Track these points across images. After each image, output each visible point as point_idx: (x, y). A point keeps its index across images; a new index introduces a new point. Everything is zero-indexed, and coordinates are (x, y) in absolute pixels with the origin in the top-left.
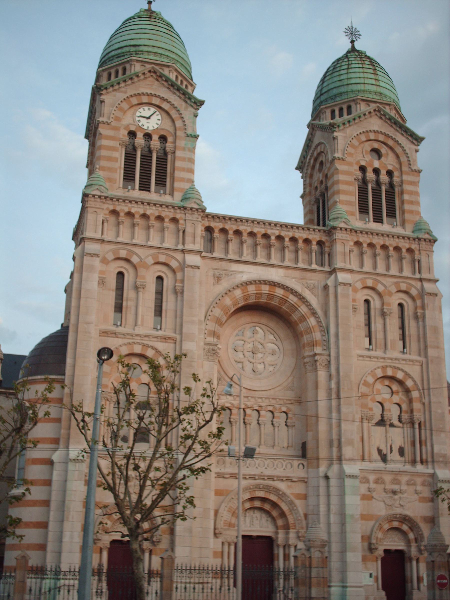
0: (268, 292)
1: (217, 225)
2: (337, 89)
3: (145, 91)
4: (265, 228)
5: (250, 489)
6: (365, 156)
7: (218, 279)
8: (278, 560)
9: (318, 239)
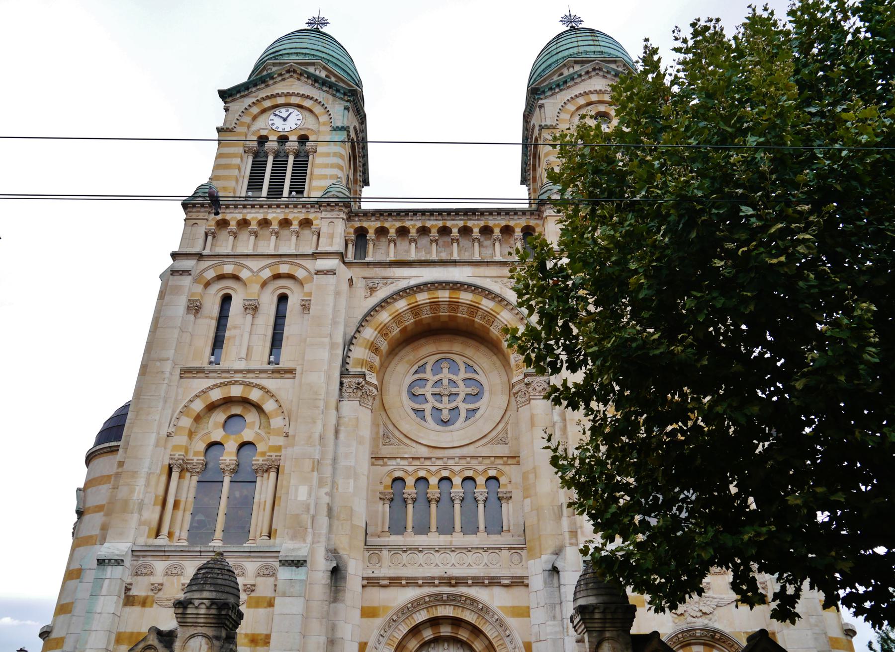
3: (280, 92)
5: (426, 602)
7: (372, 290)
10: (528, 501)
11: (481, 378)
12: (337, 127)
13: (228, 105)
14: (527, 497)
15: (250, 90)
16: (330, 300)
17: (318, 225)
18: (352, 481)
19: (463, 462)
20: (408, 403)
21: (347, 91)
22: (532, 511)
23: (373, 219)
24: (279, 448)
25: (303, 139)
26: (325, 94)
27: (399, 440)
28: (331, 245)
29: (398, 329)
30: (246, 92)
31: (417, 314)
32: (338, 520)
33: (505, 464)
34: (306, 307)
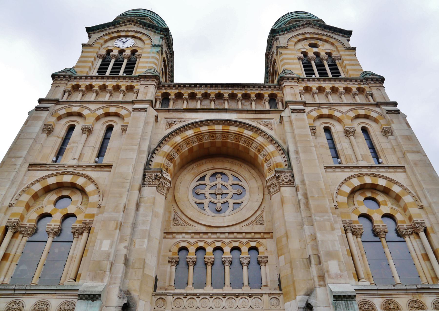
4: (218, 89)
7: (171, 125)
10: (282, 258)
11: (244, 184)
12: (155, 45)
14: (281, 255)
15: (105, 29)
16: (141, 125)
18: (146, 240)
19: (231, 236)
20: (192, 198)
21: (162, 29)
22: (285, 264)
23: (174, 88)
24: (93, 216)
26: (149, 32)
27: (185, 222)
29: (187, 148)
30: (103, 30)
31: (200, 139)
32: (133, 268)
33: (263, 238)
34: (124, 130)
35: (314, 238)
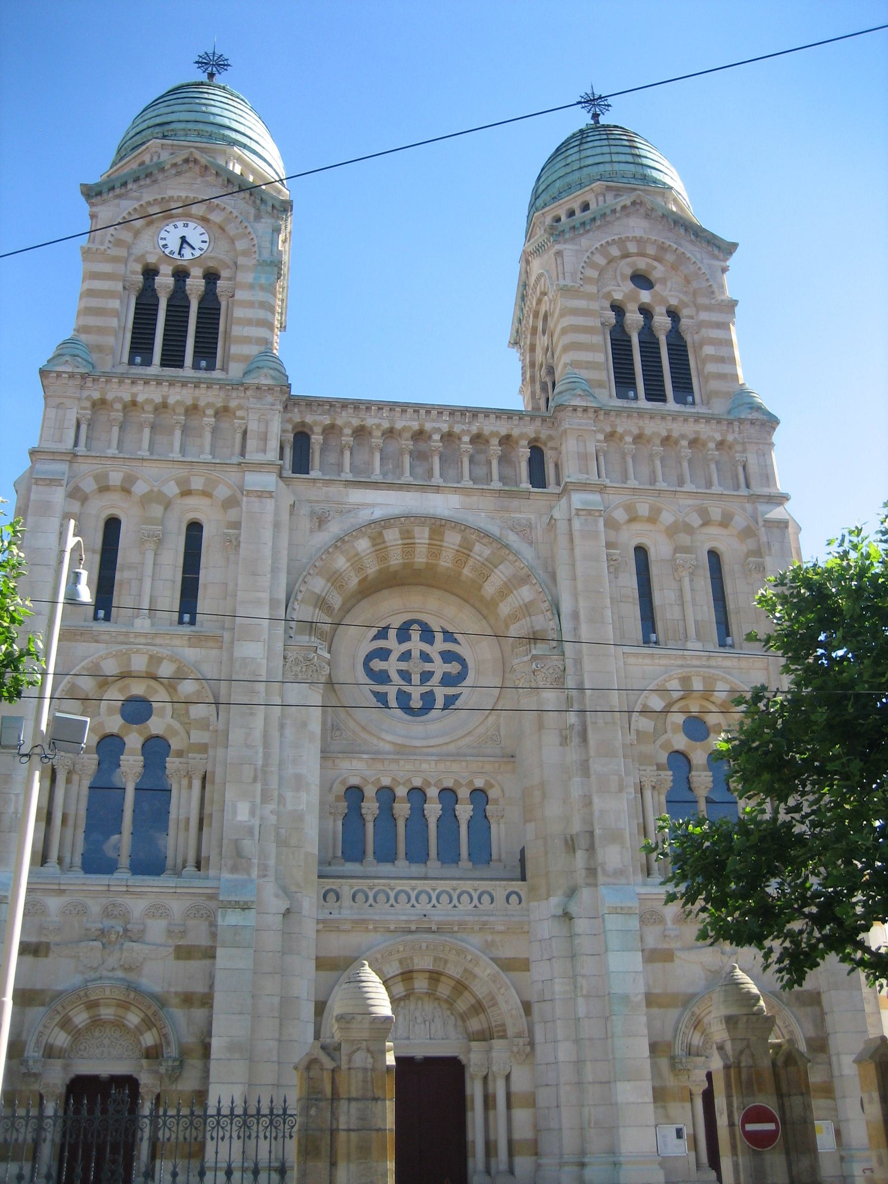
0: (427, 541)
1: (317, 420)
2: (561, 179)
6: (620, 283)
8: (473, 1109)
9: (533, 435)
10: (531, 826)
13: (95, 209)
14: (531, 821)
17: (242, 418)
25: (211, 277)
28: (264, 451)
35: (588, 803)
